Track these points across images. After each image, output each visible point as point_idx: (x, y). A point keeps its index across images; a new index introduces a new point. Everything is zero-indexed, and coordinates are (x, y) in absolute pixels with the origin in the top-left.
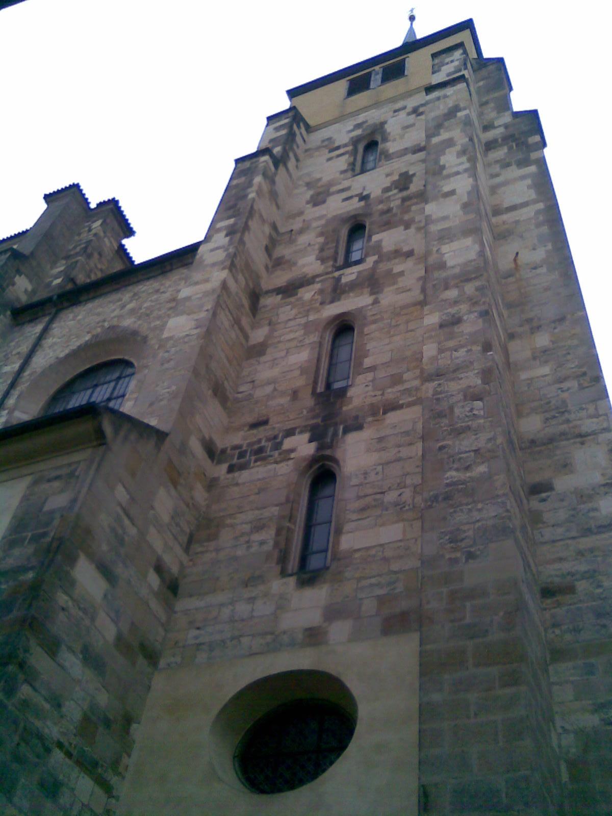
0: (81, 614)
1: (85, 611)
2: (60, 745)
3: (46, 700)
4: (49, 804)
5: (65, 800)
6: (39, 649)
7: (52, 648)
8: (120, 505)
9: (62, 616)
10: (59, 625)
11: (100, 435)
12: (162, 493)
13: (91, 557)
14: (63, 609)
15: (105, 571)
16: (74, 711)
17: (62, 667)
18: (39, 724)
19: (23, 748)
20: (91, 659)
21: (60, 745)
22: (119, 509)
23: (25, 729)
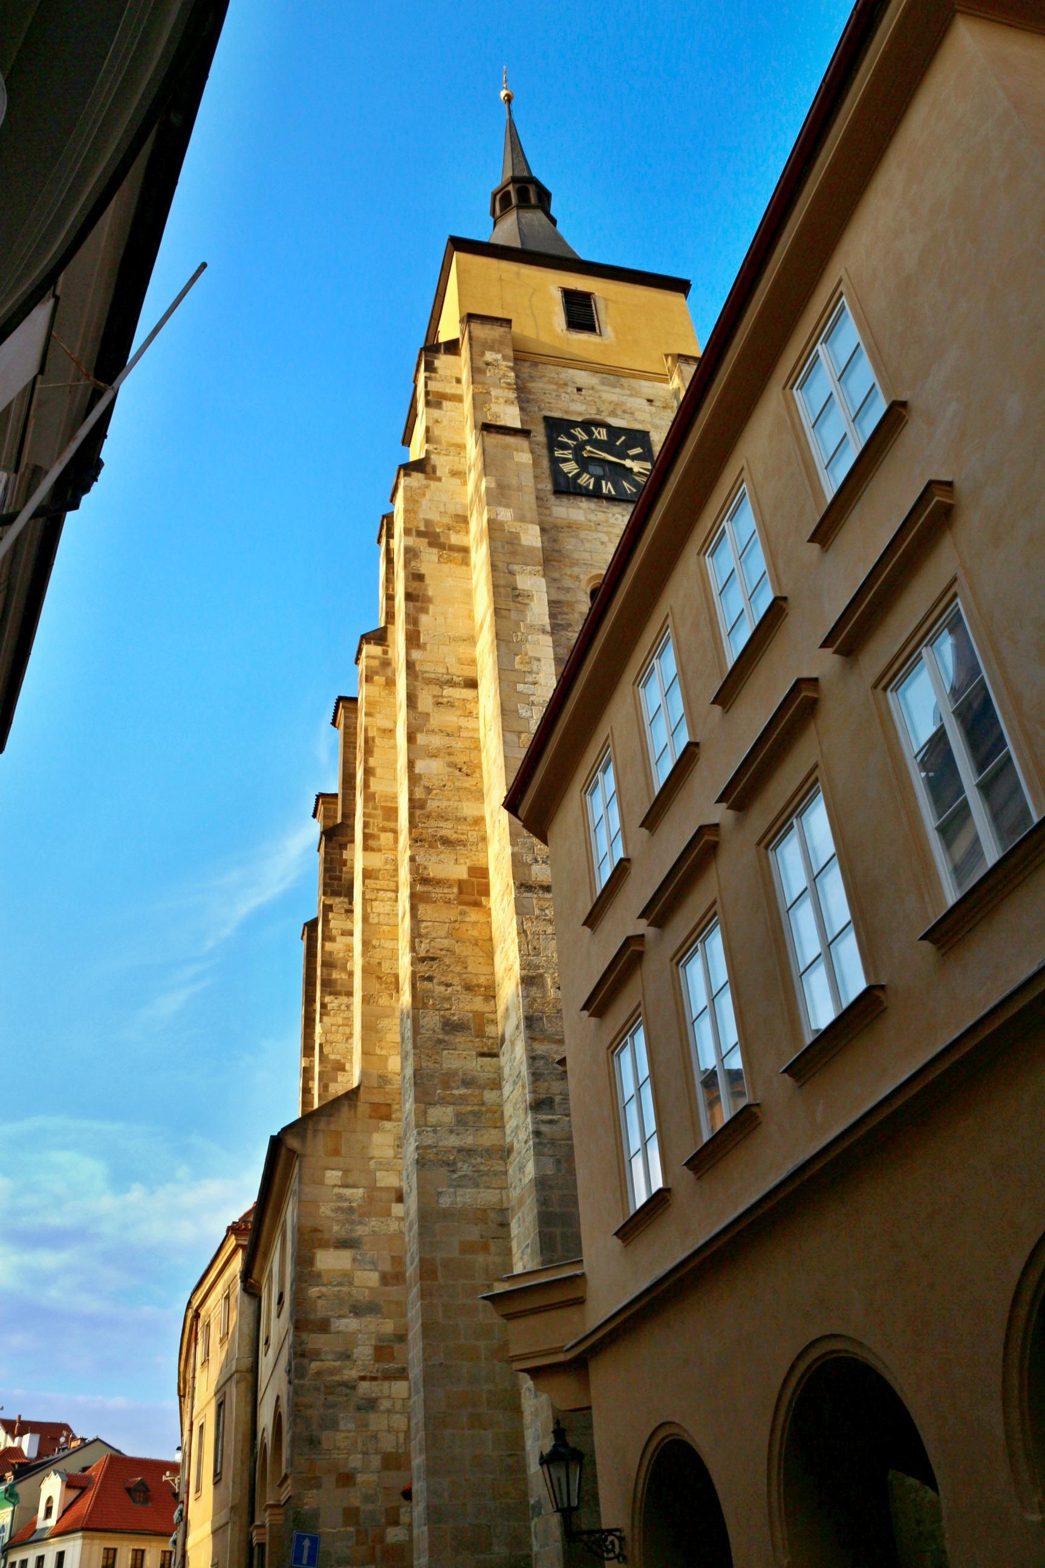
0: (337, 1289)
1: (340, 1284)
2: (363, 1378)
3: (334, 1361)
4: (372, 1416)
5: (385, 1404)
6: (312, 1335)
7: (324, 1326)
8: (335, 1186)
9: (320, 1303)
10: (322, 1309)
11: (292, 1152)
12: (377, 1138)
13: (325, 1245)
14: (319, 1297)
15: (344, 1244)
16: (364, 1352)
17: (339, 1332)
18: (337, 1378)
19: (330, 1398)
20: (357, 1310)
21: (363, 1378)
22: (337, 1190)
23: (326, 1387)
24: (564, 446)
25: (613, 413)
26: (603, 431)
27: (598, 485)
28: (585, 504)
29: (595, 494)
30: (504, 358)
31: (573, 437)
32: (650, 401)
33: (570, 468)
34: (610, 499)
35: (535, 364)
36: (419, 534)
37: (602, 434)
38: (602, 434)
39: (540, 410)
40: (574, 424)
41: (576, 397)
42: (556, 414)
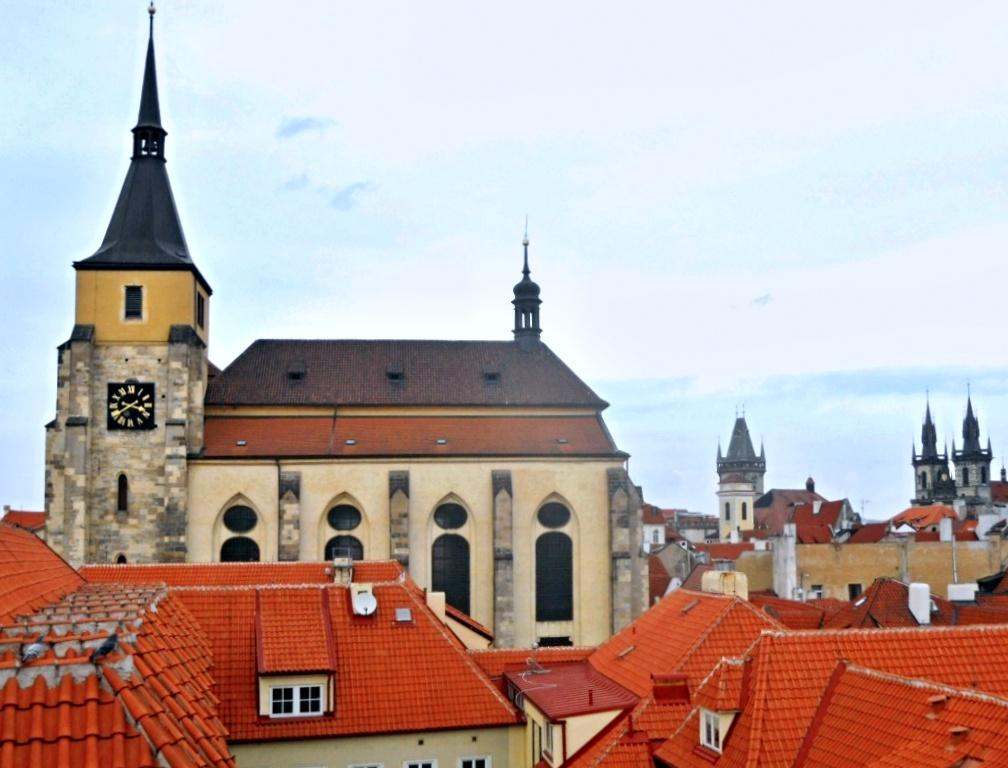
24: (114, 401)
25: (140, 373)
26: (133, 388)
27: (126, 422)
28: (120, 433)
29: (124, 428)
30: (86, 365)
31: (119, 394)
32: (159, 360)
33: (116, 414)
34: (131, 428)
35: (107, 348)
36: (52, 463)
37: (132, 390)
38: (132, 390)
39: (108, 377)
40: (119, 386)
41: (125, 365)
42: (114, 380)
